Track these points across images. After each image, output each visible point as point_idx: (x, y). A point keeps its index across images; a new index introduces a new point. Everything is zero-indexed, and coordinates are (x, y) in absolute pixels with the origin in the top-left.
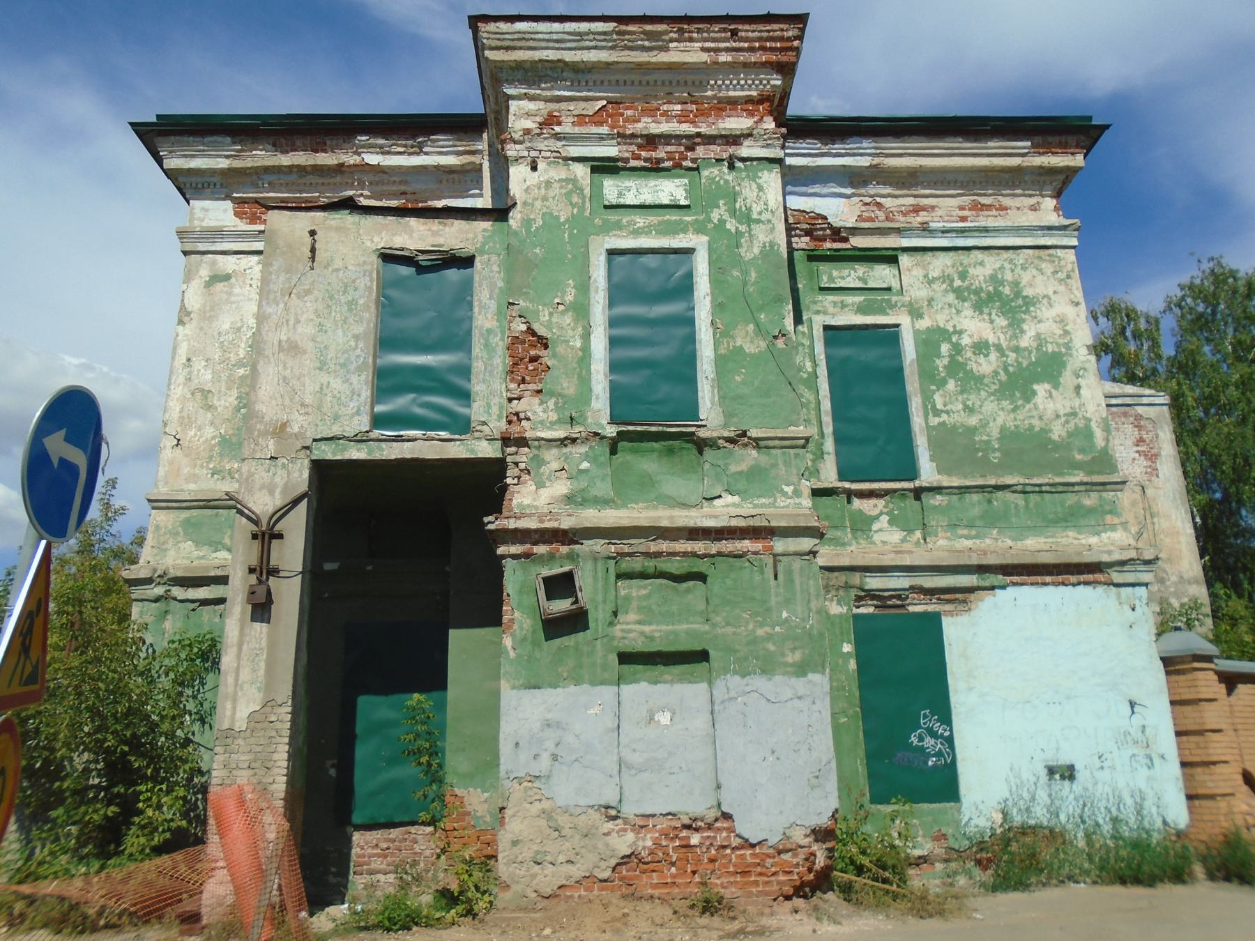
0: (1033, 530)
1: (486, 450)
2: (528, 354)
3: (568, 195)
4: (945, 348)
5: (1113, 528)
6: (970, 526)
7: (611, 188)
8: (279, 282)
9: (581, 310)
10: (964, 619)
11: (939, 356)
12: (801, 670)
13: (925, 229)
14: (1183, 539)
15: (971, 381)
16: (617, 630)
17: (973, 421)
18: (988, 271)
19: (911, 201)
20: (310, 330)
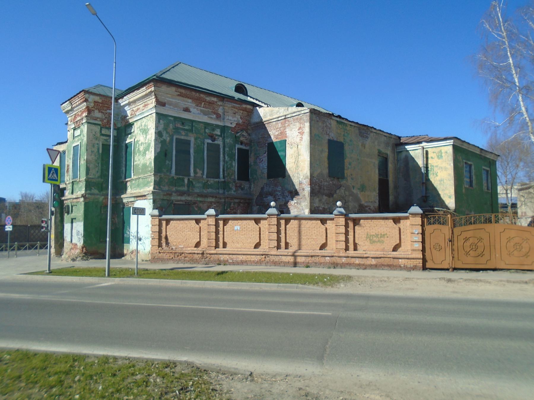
7: (77, 133)
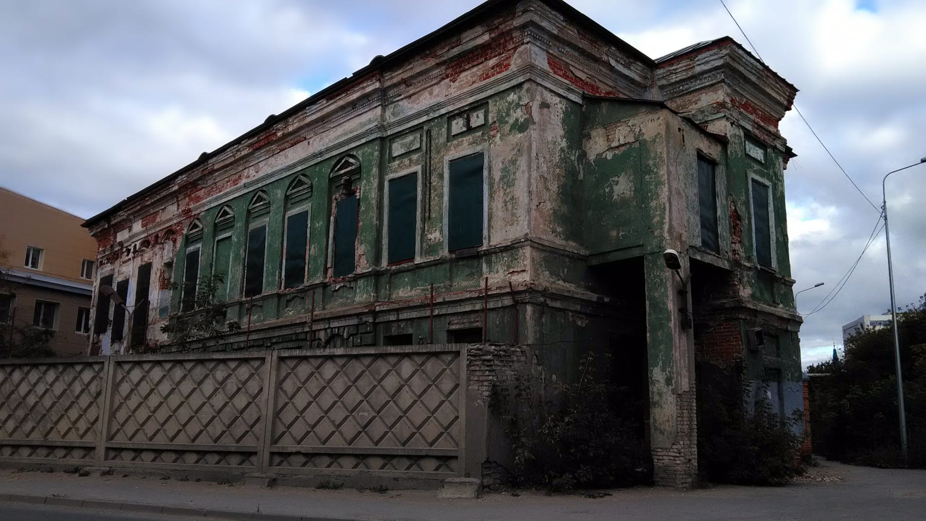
1: (726, 265)
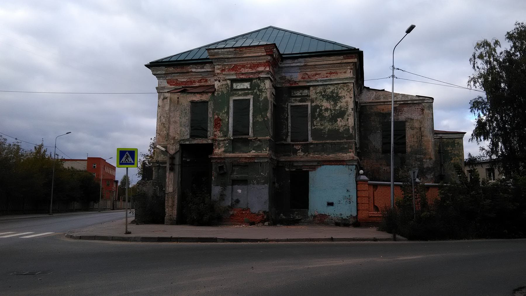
0: (333, 153)
1: (210, 142)
2: (218, 123)
3: (226, 88)
4: (318, 110)
5: (350, 152)
6: (318, 152)
8: (172, 109)
9: (228, 113)
10: (314, 172)
11: (316, 112)
12: (264, 184)
13: (317, 81)
14: (430, 143)
15: (323, 118)
16: (232, 176)
17: (322, 128)
18: (331, 90)
19: (314, 72)
20: (179, 118)
